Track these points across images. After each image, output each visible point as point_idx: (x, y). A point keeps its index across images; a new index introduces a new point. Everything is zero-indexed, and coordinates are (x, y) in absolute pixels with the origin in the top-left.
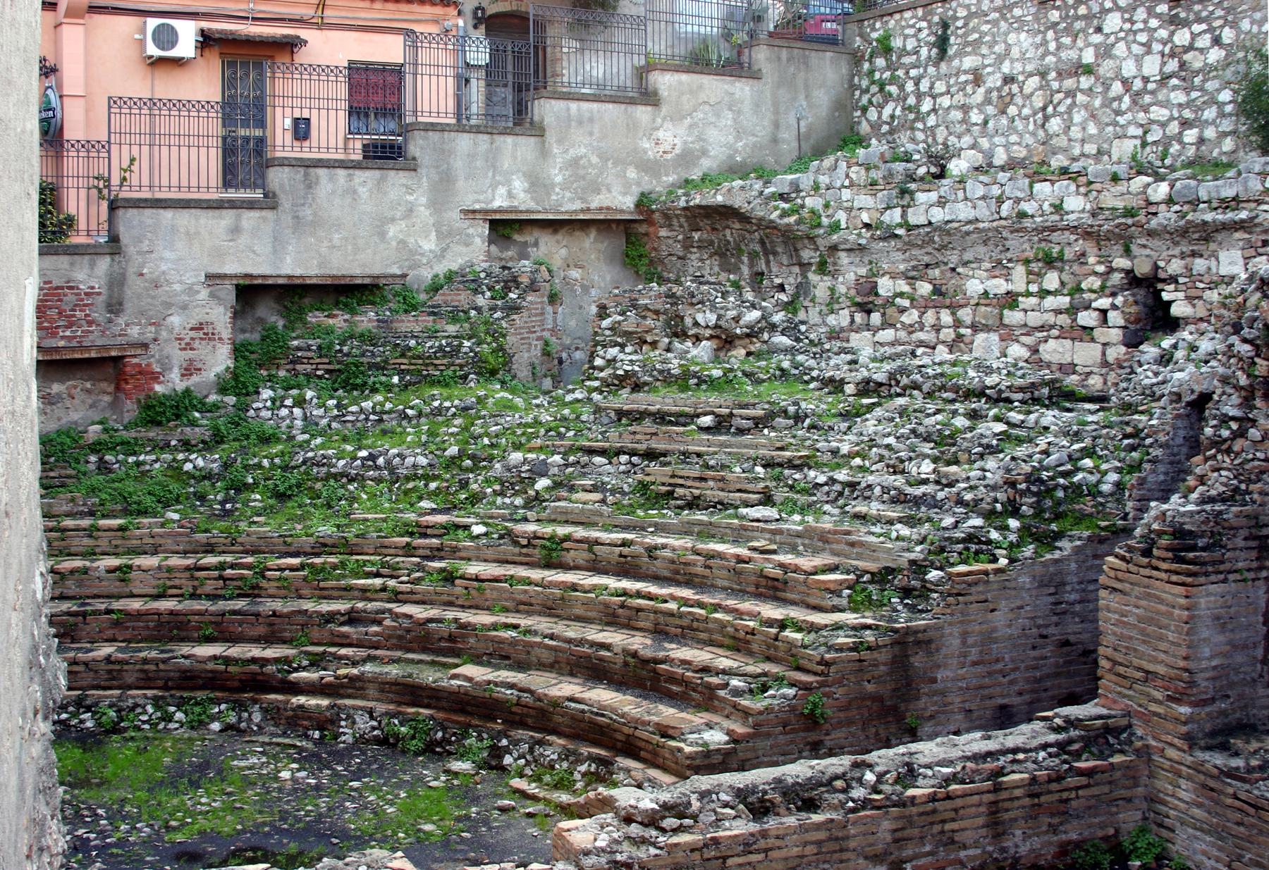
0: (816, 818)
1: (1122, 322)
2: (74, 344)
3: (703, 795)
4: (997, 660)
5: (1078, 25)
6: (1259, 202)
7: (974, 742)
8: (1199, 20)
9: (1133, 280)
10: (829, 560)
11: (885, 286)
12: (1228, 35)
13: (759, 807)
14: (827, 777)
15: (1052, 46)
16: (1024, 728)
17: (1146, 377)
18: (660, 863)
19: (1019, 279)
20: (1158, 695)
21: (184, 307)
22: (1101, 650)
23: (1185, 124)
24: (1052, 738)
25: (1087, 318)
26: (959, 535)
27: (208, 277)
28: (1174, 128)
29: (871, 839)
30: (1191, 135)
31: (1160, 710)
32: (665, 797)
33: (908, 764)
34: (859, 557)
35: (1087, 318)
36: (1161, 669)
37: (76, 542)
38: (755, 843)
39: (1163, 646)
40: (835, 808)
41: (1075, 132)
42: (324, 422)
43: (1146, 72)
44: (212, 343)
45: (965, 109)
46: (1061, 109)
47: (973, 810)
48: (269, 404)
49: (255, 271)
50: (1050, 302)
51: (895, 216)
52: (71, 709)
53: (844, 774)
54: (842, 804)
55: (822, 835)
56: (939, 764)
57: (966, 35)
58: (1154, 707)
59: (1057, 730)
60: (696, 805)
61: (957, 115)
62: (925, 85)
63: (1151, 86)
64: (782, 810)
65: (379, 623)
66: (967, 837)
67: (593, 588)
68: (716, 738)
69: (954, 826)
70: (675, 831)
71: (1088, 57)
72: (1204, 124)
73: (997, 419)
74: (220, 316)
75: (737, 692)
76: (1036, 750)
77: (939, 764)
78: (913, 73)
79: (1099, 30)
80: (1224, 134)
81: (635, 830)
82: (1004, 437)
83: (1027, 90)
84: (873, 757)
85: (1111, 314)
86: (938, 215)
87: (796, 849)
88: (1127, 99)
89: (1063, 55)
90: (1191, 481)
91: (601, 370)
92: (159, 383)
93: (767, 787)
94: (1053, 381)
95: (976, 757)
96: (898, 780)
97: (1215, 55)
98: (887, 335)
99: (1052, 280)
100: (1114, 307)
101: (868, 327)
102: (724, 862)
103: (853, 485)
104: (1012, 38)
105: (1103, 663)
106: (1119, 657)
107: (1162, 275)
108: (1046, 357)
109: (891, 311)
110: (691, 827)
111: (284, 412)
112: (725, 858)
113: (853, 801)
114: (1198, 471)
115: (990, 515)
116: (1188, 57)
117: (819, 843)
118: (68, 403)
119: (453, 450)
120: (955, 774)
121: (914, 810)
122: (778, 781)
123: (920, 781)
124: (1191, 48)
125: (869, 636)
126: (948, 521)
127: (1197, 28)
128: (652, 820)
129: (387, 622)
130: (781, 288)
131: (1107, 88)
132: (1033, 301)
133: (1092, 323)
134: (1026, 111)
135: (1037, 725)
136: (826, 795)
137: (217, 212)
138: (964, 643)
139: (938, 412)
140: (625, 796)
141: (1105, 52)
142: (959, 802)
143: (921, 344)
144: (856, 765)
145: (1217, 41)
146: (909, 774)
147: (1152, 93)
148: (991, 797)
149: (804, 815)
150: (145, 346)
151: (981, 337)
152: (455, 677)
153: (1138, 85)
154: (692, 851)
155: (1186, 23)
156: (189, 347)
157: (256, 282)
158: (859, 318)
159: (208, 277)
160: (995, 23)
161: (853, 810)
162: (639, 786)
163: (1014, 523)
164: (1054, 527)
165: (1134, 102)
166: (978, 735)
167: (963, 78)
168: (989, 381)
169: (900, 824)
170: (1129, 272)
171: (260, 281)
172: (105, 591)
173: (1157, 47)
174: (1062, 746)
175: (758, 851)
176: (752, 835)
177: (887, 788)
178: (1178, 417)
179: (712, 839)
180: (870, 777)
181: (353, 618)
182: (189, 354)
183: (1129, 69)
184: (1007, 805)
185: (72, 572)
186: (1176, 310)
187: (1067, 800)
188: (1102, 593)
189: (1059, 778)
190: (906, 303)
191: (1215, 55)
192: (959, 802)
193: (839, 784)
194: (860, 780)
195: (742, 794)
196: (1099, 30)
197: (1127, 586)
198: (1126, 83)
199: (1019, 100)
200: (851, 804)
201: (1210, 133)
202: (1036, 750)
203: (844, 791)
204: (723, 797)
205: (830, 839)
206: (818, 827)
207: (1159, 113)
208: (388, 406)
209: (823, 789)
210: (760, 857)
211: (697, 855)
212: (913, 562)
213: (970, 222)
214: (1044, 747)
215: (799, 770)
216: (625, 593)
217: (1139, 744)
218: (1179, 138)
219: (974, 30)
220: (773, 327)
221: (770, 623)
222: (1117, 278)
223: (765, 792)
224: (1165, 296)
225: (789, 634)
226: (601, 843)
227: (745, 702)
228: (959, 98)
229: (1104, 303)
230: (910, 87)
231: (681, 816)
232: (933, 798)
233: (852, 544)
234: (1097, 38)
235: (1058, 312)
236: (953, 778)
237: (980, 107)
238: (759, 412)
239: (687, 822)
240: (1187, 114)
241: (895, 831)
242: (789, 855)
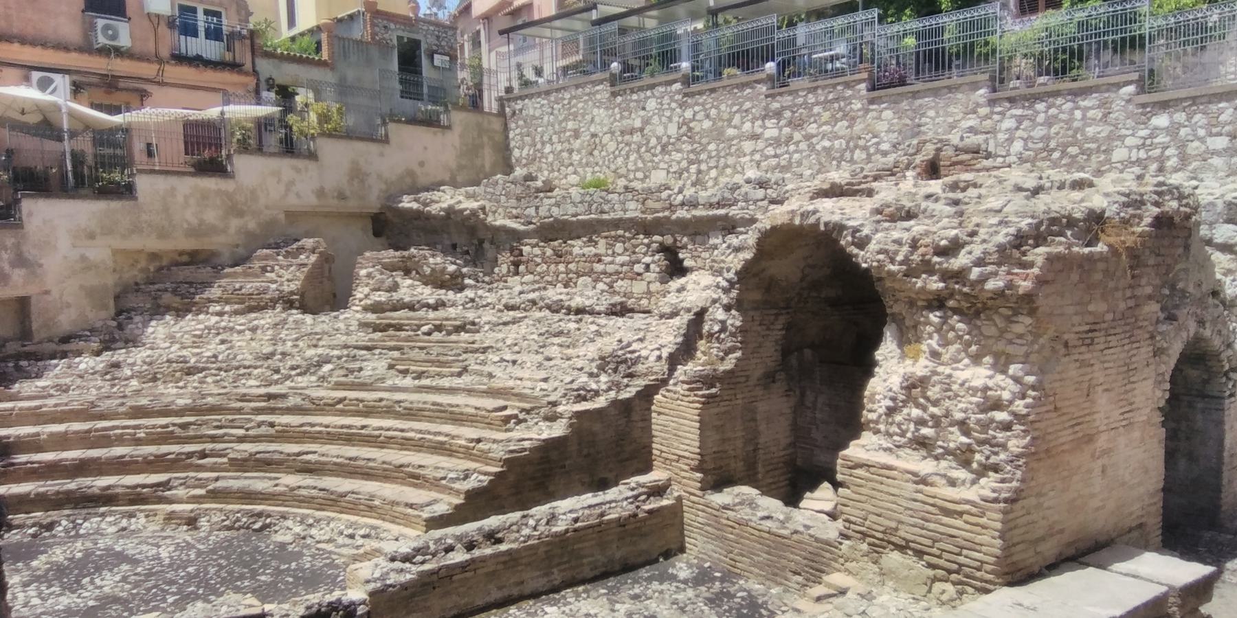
0: (503, 547)
1: (658, 269)
3: (437, 541)
4: (598, 453)
5: (632, 105)
6: (730, 206)
7: (589, 498)
8: (697, 104)
9: (663, 249)
10: (501, 403)
11: (526, 249)
12: (713, 112)
13: (470, 546)
15: (618, 116)
16: (615, 489)
17: (672, 298)
19: (602, 247)
20: (686, 468)
22: (654, 445)
23: (691, 162)
24: (630, 494)
25: (638, 268)
26: (575, 386)
28: (684, 164)
30: (693, 168)
31: (687, 475)
32: (415, 544)
34: (520, 401)
35: (638, 268)
36: (686, 454)
39: (687, 442)
40: (514, 541)
41: (631, 166)
42: (179, 335)
43: (669, 133)
45: (570, 151)
46: (623, 153)
50: (619, 259)
51: (532, 211)
55: (507, 558)
56: (570, 512)
57: (570, 109)
58: (683, 474)
59: (633, 489)
60: (432, 547)
61: (565, 155)
62: (546, 138)
63: (672, 140)
65: (225, 456)
67: (363, 427)
68: (442, 508)
69: (580, 546)
70: (423, 563)
71: (638, 124)
72: (699, 162)
73: (592, 323)
75: (453, 480)
76: (623, 500)
77: (570, 512)
78: (540, 129)
79: (644, 109)
80: (711, 168)
81: (398, 565)
82: (598, 333)
83: (604, 142)
84: (533, 511)
85: (652, 266)
86: (556, 211)
88: (659, 148)
89: (625, 122)
90: (699, 354)
91: (361, 300)
94: (621, 303)
95: (590, 507)
96: (547, 523)
97: (707, 124)
98: (529, 278)
99: (619, 247)
100: (653, 262)
101: (517, 273)
103: (514, 362)
104: (596, 111)
105: (655, 452)
106: (664, 449)
107: (679, 244)
108: (617, 289)
109: (531, 265)
114: (702, 349)
115: (591, 375)
116: (692, 125)
117: (504, 563)
119: (267, 349)
122: (480, 529)
123: (560, 523)
124: (694, 119)
125: (527, 444)
126: (569, 379)
127: (697, 108)
128: (407, 559)
129: (231, 456)
130: (467, 253)
131: (648, 142)
132: (609, 259)
133: (642, 271)
134: (604, 153)
135: (621, 487)
138: (579, 444)
139: (560, 320)
140: (389, 547)
141: (646, 122)
142: (582, 533)
143: (550, 283)
144: (524, 517)
145: (708, 116)
146: (552, 519)
147: (673, 144)
149: (495, 547)
151: (581, 280)
152: (276, 485)
153: (665, 139)
155: (691, 106)
158: (512, 268)
160: (586, 102)
162: (397, 540)
163: (604, 378)
164: (626, 380)
165: (663, 149)
166: (590, 495)
167: (568, 134)
168: (587, 303)
170: (661, 244)
173: (676, 119)
174: (636, 497)
178: (690, 321)
180: (532, 522)
181: (203, 455)
183: (660, 130)
186: (687, 263)
187: (639, 528)
188: (654, 415)
189: (635, 515)
190: (538, 260)
191: (707, 124)
193: (514, 528)
194: (526, 525)
195: (459, 538)
196: (644, 109)
197: (667, 411)
198: (659, 138)
199: (599, 148)
201: (703, 167)
202: (623, 500)
204: (449, 541)
207: (678, 156)
208: (223, 324)
211: (435, 577)
212: (549, 403)
213: (574, 216)
214: (627, 499)
215: (493, 522)
216: (381, 428)
217: (676, 494)
218: (687, 170)
219: (575, 106)
220: (463, 276)
221: (472, 441)
222: (655, 246)
224: (681, 256)
225: (481, 445)
226: (377, 575)
227: (457, 486)
228: (566, 145)
229: (647, 259)
230: (538, 139)
232: (567, 531)
233: (516, 395)
234: (642, 113)
235: (622, 265)
236: (576, 520)
237: (579, 151)
238: (458, 323)
239: (428, 557)
240: (692, 156)
241: (546, 552)
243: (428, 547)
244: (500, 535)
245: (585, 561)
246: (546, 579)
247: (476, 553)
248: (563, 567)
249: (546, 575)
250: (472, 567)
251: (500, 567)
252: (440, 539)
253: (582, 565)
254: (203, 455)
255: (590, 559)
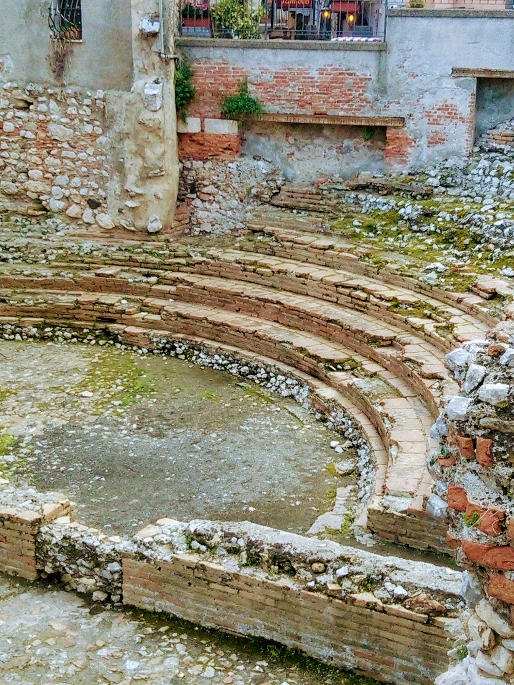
0: (285, 581)
2: (350, 114)
14: (311, 558)
18: (167, 567)
21: (434, 93)
27: (454, 70)
29: (317, 614)
33: (383, 575)
37: (299, 252)
38: (230, 580)
44: (455, 121)
47: (407, 631)
48: (481, 172)
49: (493, 68)
52: (230, 359)
53: (328, 561)
54: (306, 581)
56: (404, 586)
60: (216, 539)
64: (265, 566)
66: (401, 649)
70: (198, 551)
74: (463, 100)
87: (259, 597)
92: (411, 147)
93: (266, 547)
102: (208, 584)
110: (204, 553)
111: (488, 179)
112: (209, 582)
113: (316, 583)
117: (277, 600)
118: (354, 153)
120: (407, 597)
121: (354, 609)
136: (302, 570)
137: (463, 20)
142: (394, 620)
148: (425, 628)
150: (402, 120)
154: (188, 567)
156: (436, 122)
157: (494, 76)
159: (454, 70)
161: (310, 589)
169: (340, 614)
171: (498, 76)
172: (294, 289)
175: (232, 587)
176: (229, 574)
177: (347, 584)
179: (202, 565)
180: (343, 571)
182: (436, 128)
184: (437, 639)
185: (279, 272)
192: (394, 620)
194: (335, 570)
200: (312, 584)
203: (317, 573)
204: (242, 543)
205: (284, 601)
206: (278, 589)
209: (302, 565)
210: (235, 591)
223: (262, 551)
231: (203, 543)
236: (399, 600)
239: (203, 548)
241: (338, 617)
242: (254, 598)
243: (211, 537)
244: (295, 566)
245: (395, 660)
246: (332, 652)
247: (247, 571)
248: (360, 650)
249: (335, 647)
250: (235, 583)
251: (270, 602)
252: (232, 535)
253: (390, 664)
254: (391, 343)
255: (404, 663)
